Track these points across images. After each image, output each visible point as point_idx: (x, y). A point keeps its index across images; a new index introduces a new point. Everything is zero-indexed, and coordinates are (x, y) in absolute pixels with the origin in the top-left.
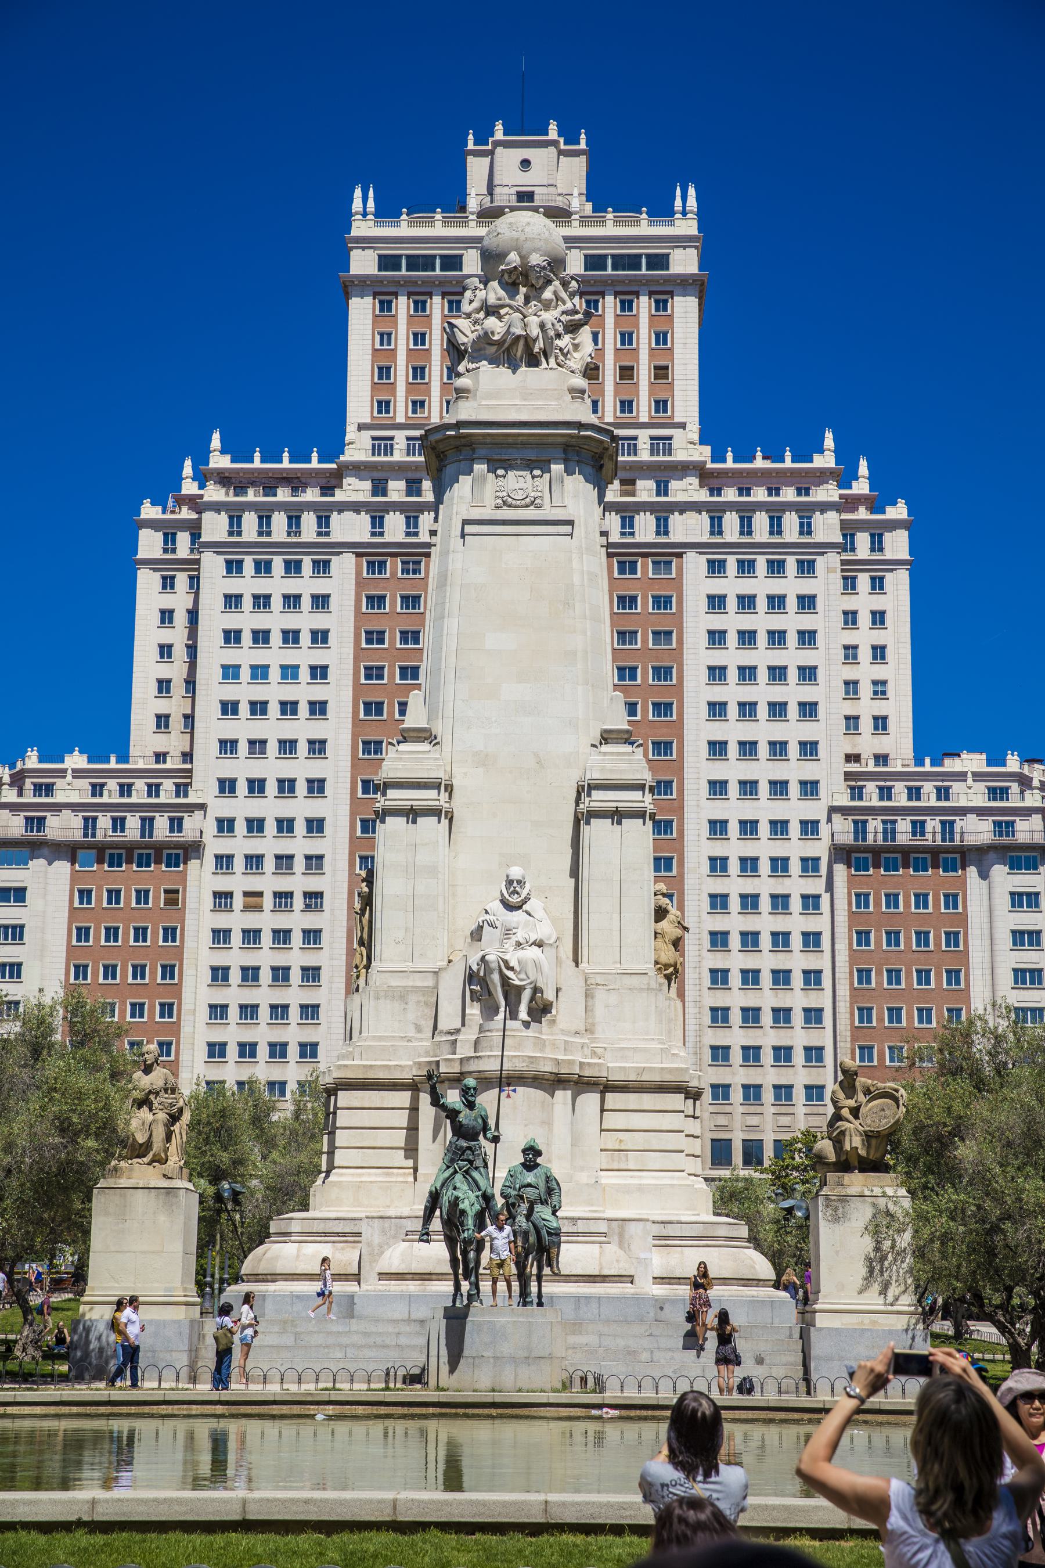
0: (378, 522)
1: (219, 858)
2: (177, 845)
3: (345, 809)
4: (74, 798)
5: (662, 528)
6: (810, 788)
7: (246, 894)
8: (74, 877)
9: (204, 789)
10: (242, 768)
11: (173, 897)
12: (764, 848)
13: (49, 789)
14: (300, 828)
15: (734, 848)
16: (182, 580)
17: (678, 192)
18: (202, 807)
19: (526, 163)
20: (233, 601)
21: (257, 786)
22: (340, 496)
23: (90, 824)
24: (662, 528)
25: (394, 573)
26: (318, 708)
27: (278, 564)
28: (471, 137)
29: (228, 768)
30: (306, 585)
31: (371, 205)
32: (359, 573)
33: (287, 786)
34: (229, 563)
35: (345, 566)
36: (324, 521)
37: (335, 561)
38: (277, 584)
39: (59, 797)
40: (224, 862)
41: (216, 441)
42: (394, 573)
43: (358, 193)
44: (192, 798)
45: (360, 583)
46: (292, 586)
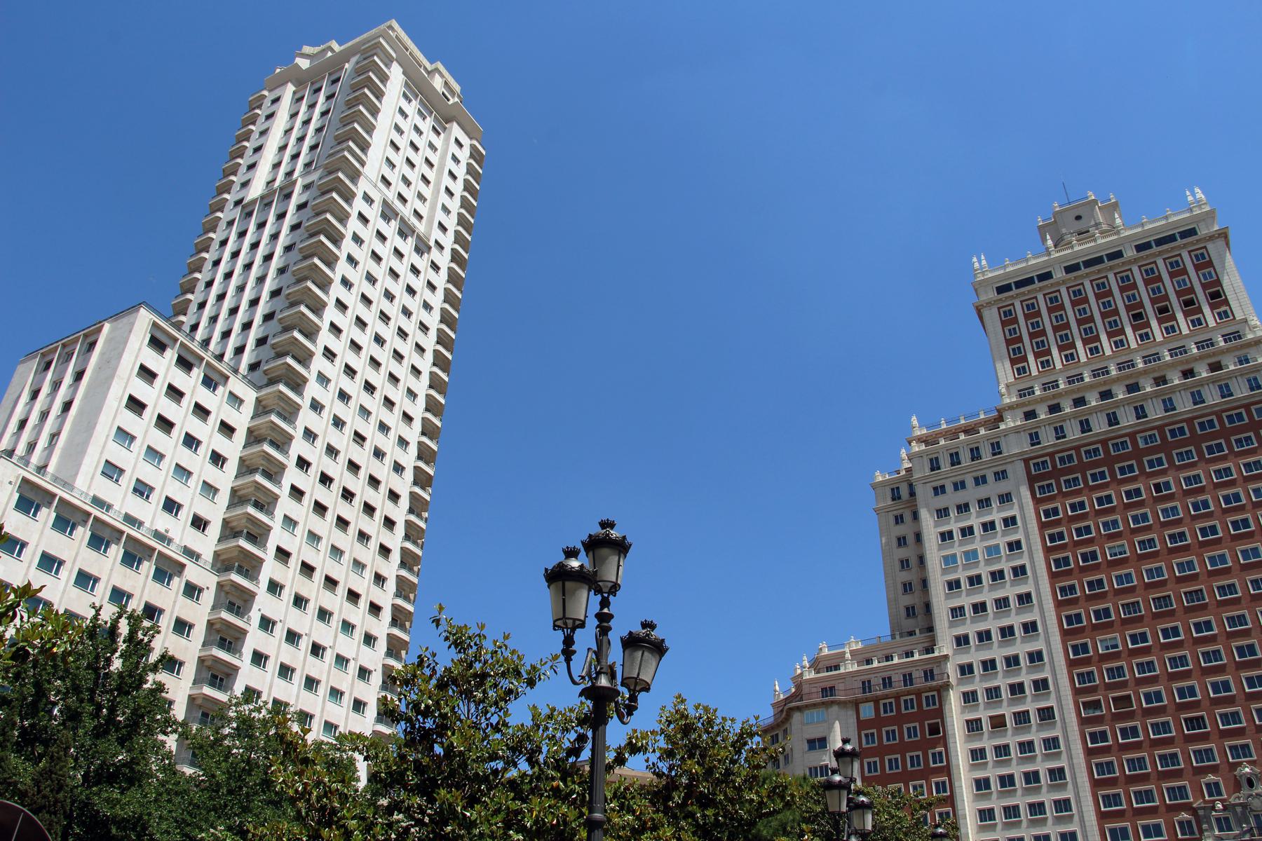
0: (1035, 439)
1: (965, 695)
2: (931, 689)
4: (856, 668)
7: (991, 718)
8: (862, 725)
9: (945, 647)
11: (934, 730)
13: (837, 667)
14: (1024, 661)
16: (908, 516)
17: (1188, 193)
18: (946, 657)
19: (1078, 218)
20: (942, 513)
22: (1002, 426)
23: (866, 686)
25: (1054, 466)
26: (1019, 571)
27: (970, 482)
30: (993, 489)
31: (984, 262)
34: (935, 489)
35: (1017, 472)
36: (996, 448)
37: (1009, 469)
38: (972, 494)
39: (842, 670)
40: (969, 697)
42: (1054, 466)
43: (975, 259)
44: (936, 654)
46: (983, 492)
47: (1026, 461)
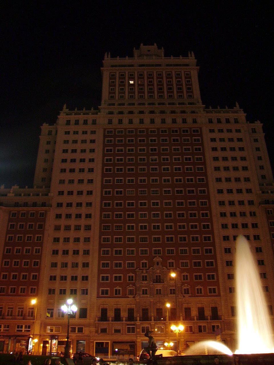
3: (98, 199)
5: (195, 121)
6: (249, 191)
10: (67, 187)
12: (237, 209)
15: (228, 209)
17: (189, 53)
19: (149, 51)
21: (70, 193)
24: (195, 121)
25: (115, 133)
28: (134, 49)
29: (61, 188)
31: (109, 56)
32: (104, 133)
33: (80, 193)
36: (94, 122)
41: (65, 106)
45: (105, 136)
47: (105, 129)
